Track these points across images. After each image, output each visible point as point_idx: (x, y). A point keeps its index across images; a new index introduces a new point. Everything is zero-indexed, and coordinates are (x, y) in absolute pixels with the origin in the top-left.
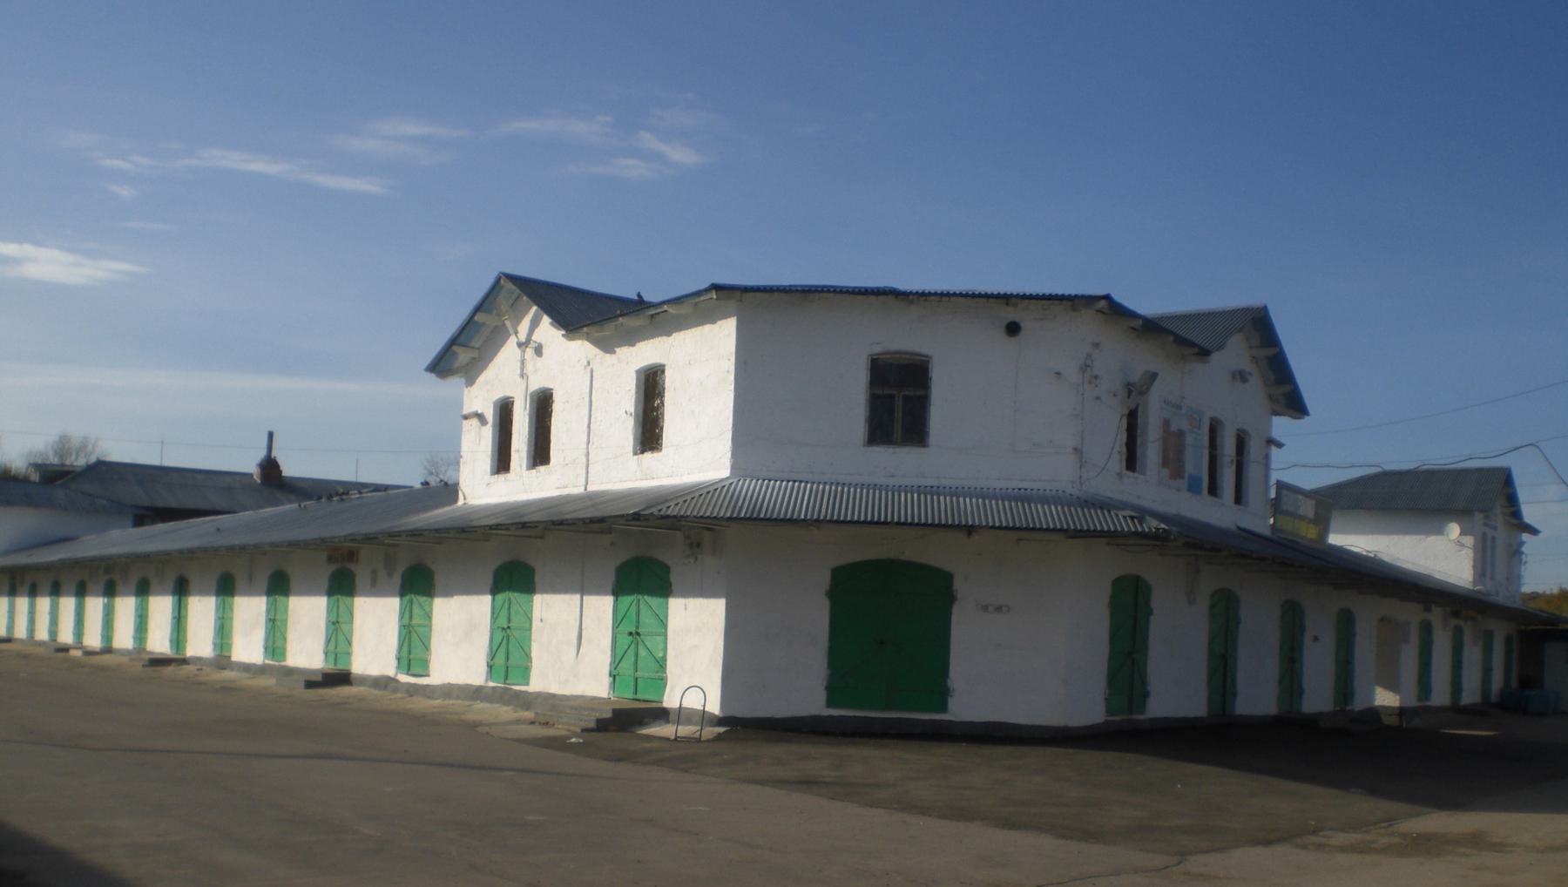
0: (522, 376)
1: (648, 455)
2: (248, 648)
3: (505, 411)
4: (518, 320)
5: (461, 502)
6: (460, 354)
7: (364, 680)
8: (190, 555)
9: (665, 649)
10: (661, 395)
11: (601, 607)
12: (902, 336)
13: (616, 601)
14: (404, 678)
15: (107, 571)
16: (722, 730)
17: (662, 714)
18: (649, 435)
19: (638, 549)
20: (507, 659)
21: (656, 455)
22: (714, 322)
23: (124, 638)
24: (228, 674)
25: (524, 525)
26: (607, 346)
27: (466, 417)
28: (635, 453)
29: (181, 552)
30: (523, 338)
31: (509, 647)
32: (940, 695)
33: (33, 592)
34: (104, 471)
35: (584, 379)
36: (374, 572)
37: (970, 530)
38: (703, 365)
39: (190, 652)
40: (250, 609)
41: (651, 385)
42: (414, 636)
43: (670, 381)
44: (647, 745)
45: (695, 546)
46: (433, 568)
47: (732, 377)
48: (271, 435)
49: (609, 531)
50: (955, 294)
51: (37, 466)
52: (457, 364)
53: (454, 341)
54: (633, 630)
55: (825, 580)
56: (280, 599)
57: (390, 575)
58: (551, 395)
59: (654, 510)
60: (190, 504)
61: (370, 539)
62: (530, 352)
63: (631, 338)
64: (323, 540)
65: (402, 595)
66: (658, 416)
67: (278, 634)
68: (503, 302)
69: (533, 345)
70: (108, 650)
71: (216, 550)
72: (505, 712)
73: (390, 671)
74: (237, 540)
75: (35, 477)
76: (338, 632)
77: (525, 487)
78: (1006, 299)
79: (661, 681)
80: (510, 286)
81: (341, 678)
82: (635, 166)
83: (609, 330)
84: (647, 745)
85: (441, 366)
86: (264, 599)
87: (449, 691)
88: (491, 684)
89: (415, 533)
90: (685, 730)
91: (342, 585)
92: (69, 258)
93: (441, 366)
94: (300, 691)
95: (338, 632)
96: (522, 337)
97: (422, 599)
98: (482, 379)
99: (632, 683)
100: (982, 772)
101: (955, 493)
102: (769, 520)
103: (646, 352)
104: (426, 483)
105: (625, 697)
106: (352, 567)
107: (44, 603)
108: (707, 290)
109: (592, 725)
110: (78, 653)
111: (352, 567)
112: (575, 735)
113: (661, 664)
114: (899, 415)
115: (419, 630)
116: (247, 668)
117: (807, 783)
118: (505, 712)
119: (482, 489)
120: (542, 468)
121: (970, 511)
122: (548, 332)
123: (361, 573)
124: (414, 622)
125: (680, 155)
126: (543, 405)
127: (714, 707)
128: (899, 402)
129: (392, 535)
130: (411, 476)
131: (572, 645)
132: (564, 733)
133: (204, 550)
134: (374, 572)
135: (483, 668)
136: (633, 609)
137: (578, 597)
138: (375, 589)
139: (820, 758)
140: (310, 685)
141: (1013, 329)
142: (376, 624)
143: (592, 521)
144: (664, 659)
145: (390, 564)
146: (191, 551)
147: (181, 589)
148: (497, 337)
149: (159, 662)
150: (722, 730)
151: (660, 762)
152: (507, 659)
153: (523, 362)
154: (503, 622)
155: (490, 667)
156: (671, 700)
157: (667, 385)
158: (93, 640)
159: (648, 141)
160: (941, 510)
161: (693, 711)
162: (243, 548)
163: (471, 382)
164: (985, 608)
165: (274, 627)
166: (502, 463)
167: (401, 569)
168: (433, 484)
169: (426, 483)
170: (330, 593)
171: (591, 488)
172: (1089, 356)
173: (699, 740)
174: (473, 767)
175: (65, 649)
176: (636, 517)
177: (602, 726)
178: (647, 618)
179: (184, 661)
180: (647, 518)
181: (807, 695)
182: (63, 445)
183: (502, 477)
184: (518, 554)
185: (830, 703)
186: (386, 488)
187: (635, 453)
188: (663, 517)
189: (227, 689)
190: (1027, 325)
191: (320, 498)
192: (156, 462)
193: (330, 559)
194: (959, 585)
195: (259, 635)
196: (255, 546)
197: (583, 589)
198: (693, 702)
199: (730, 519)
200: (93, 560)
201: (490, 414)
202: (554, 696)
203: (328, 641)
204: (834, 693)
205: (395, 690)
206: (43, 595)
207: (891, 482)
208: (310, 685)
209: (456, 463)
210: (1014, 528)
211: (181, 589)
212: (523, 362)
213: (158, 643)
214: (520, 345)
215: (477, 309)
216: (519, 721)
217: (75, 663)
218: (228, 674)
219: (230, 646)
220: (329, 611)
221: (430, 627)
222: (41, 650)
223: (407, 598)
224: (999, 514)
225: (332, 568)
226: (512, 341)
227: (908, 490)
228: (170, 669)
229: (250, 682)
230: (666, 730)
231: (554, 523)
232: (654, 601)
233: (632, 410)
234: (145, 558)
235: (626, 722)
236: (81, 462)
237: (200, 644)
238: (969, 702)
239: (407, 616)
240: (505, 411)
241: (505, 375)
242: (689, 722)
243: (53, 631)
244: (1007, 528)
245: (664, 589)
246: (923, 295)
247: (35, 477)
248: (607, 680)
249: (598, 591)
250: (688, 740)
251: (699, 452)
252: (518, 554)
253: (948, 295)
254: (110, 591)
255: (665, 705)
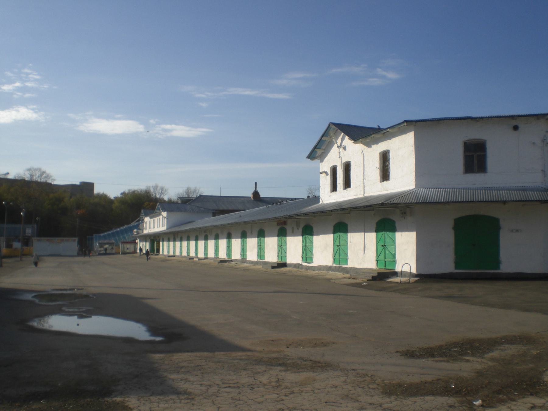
0: (339, 157)
1: (385, 182)
2: (252, 256)
3: (334, 170)
4: (337, 138)
5: (321, 203)
6: (318, 151)
7: (291, 265)
8: (232, 225)
9: (395, 251)
10: (389, 161)
11: (371, 237)
12: (474, 134)
13: (377, 234)
14: (304, 264)
15: (205, 232)
16: (417, 279)
17: (395, 274)
18: (385, 175)
19: (383, 216)
20: (340, 256)
21: (388, 182)
22: (406, 133)
23: (211, 254)
24: (246, 265)
25: (343, 209)
26: (368, 145)
27: (321, 173)
28: (381, 182)
29: (228, 224)
30: (339, 144)
31: (340, 252)
32: (497, 263)
33: (181, 240)
34: (202, 199)
35: (361, 157)
36: (293, 228)
37: (505, 202)
38: (403, 148)
39: (233, 258)
40: (252, 242)
41: (385, 157)
42: (307, 250)
43: (392, 156)
44: (391, 285)
45: (404, 213)
46: (313, 225)
47: (414, 153)
48: (256, 183)
49: (373, 210)
50: (493, 117)
51: (180, 198)
52: (317, 155)
53: (315, 147)
54: (383, 244)
55: (452, 223)
56: (262, 239)
57: (298, 229)
58: (389, 152)
59: (389, 202)
60: (235, 209)
61: (291, 217)
62: (342, 149)
63: (377, 142)
64: (275, 218)
65: (302, 236)
66: (396, 168)
67: (262, 251)
68: (331, 133)
69: (343, 146)
70: (206, 258)
71: (240, 223)
72: (340, 275)
73: (300, 262)
74: (247, 219)
75: (180, 202)
76: (282, 249)
77: (343, 196)
78: (512, 117)
79: (394, 262)
80: (333, 127)
81: (284, 265)
82: (377, 81)
83: (369, 139)
84: (391, 285)
85: (312, 156)
86: (277, 238)
87: (320, 268)
88: (335, 265)
89: (306, 214)
90: (404, 279)
91: (282, 233)
92: (188, 128)
93: (312, 156)
94: (270, 269)
95: (282, 249)
96: (339, 144)
97: (309, 237)
98: (326, 159)
99: (384, 263)
100: (514, 291)
101: (498, 189)
102: (430, 203)
103: (382, 146)
104: (309, 197)
105: (382, 268)
106: (285, 226)
107: (185, 243)
108: (403, 122)
109: (371, 278)
110: (197, 260)
111: (285, 226)
112: (365, 282)
113: (394, 256)
114: (476, 162)
115: (309, 247)
116: (252, 262)
117: (449, 297)
118: (340, 275)
119: (328, 198)
120: (348, 189)
121: (504, 195)
122: (347, 142)
123: (288, 228)
124: (307, 244)
125: (392, 75)
126: (347, 167)
127: (414, 271)
128: (475, 157)
129: (298, 215)
130: (302, 194)
131: (362, 250)
132: (361, 281)
133: (236, 223)
134: (293, 228)
135: (331, 260)
136: (383, 237)
137: (363, 233)
138: (293, 234)
139: (453, 288)
140: (273, 267)
141: (516, 128)
142: (294, 245)
143: (367, 206)
144: (395, 254)
145: (298, 226)
146: (232, 224)
147: (229, 237)
148: (330, 145)
149: (223, 261)
150: (417, 279)
151: (395, 291)
152: (340, 256)
153: (339, 153)
154: (337, 243)
155: (334, 259)
156: (398, 269)
157: (391, 157)
158: (201, 255)
159: (380, 71)
160: (493, 196)
161: (406, 272)
162: (249, 222)
163: (322, 161)
164: (512, 231)
165: (260, 248)
166: (334, 188)
167: (302, 226)
168: (311, 197)
169: (309, 197)
170: (278, 236)
171: (366, 195)
172: (545, 136)
173: (409, 283)
174: (329, 294)
175: (192, 258)
176: (382, 204)
177: (374, 278)
178: (388, 239)
179: (231, 261)
180: (386, 204)
181: (447, 265)
182: (188, 191)
183: (334, 193)
184: (342, 220)
185: (456, 268)
186: (295, 199)
187: (381, 182)
188: (392, 204)
189: (246, 270)
190: (521, 126)
191: (273, 204)
192: (218, 194)
193: (278, 224)
194: (502, 223)
195: (256, 251)
196: (253, 221)
197: (365, 231)
198: (406, 269)
199: (416, 203)
200: (200, 228)
201: (329, 172)
202: (357, 268)
203: (278, 252)
204: (457, 265)
205: (302, 268)
206: (185, 241)
207: (475, 186)
208: (273, 267)
209: (319, 189)
210: (521, 201)
211: (229, 237)
212: (339, 153)
213: (223, 255)
214: (338, 147)
215: (323, 136)
216: (345, 278)
217: (195, 263)
218: (246, 265)
219: (246, 255)
220: (334, 241)
221: (312, 246)
222: (184, 259)
223: (304, 237)
224: (515, 196)
225: (279, 227)
226: (336, 146)
227: (481, 189)
228: (227, 264)
229: (252, 267)
230: (397, 279)
231: (353, 208)
232: (390, 234)
233: (379, 167)
234: (217, 227)
235: (382, 277)
236: (195, 196)
237: (236, 255)
238: (508, 265)
239: (304, 242)
240: (334, 170)
241: (334, 158)
242: (405, 276)
243: (188, 253)
244: (519, 201)
245: (393, 229)
246: (482, 118)
247: (180, 202)
248: (374, 262)
249: (370, 231)
250: (405, 283)
251: (404, 180)
252: (342, 220)
253: (491, 117)
254: (206, 238)
255: (396, 270)
